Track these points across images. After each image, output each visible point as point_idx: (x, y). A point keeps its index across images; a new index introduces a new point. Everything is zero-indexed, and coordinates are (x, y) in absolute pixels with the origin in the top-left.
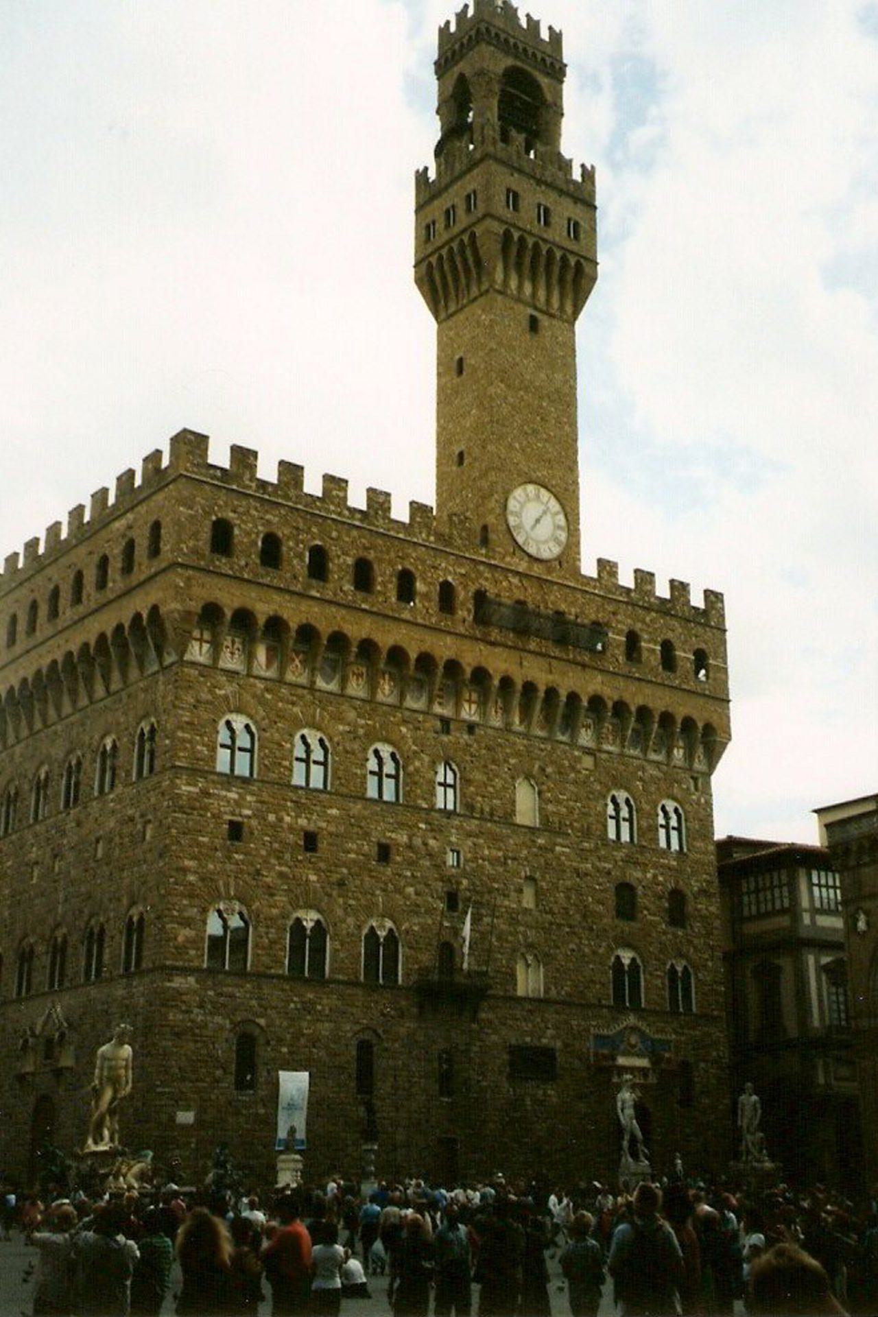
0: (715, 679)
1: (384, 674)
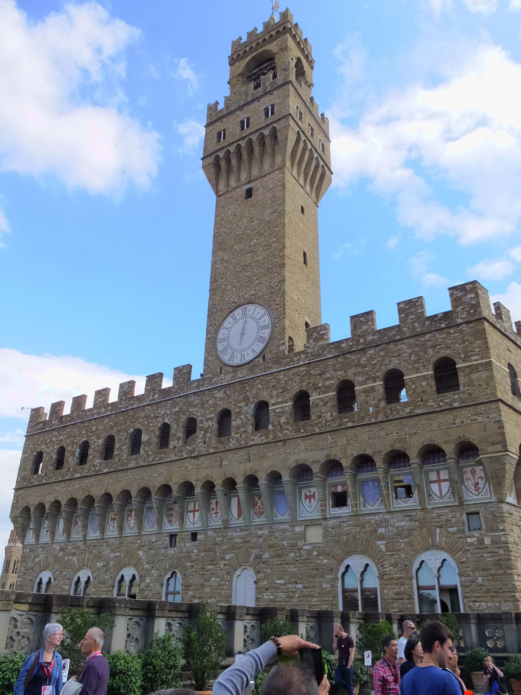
0: (470, 383)
1: (131, 511)
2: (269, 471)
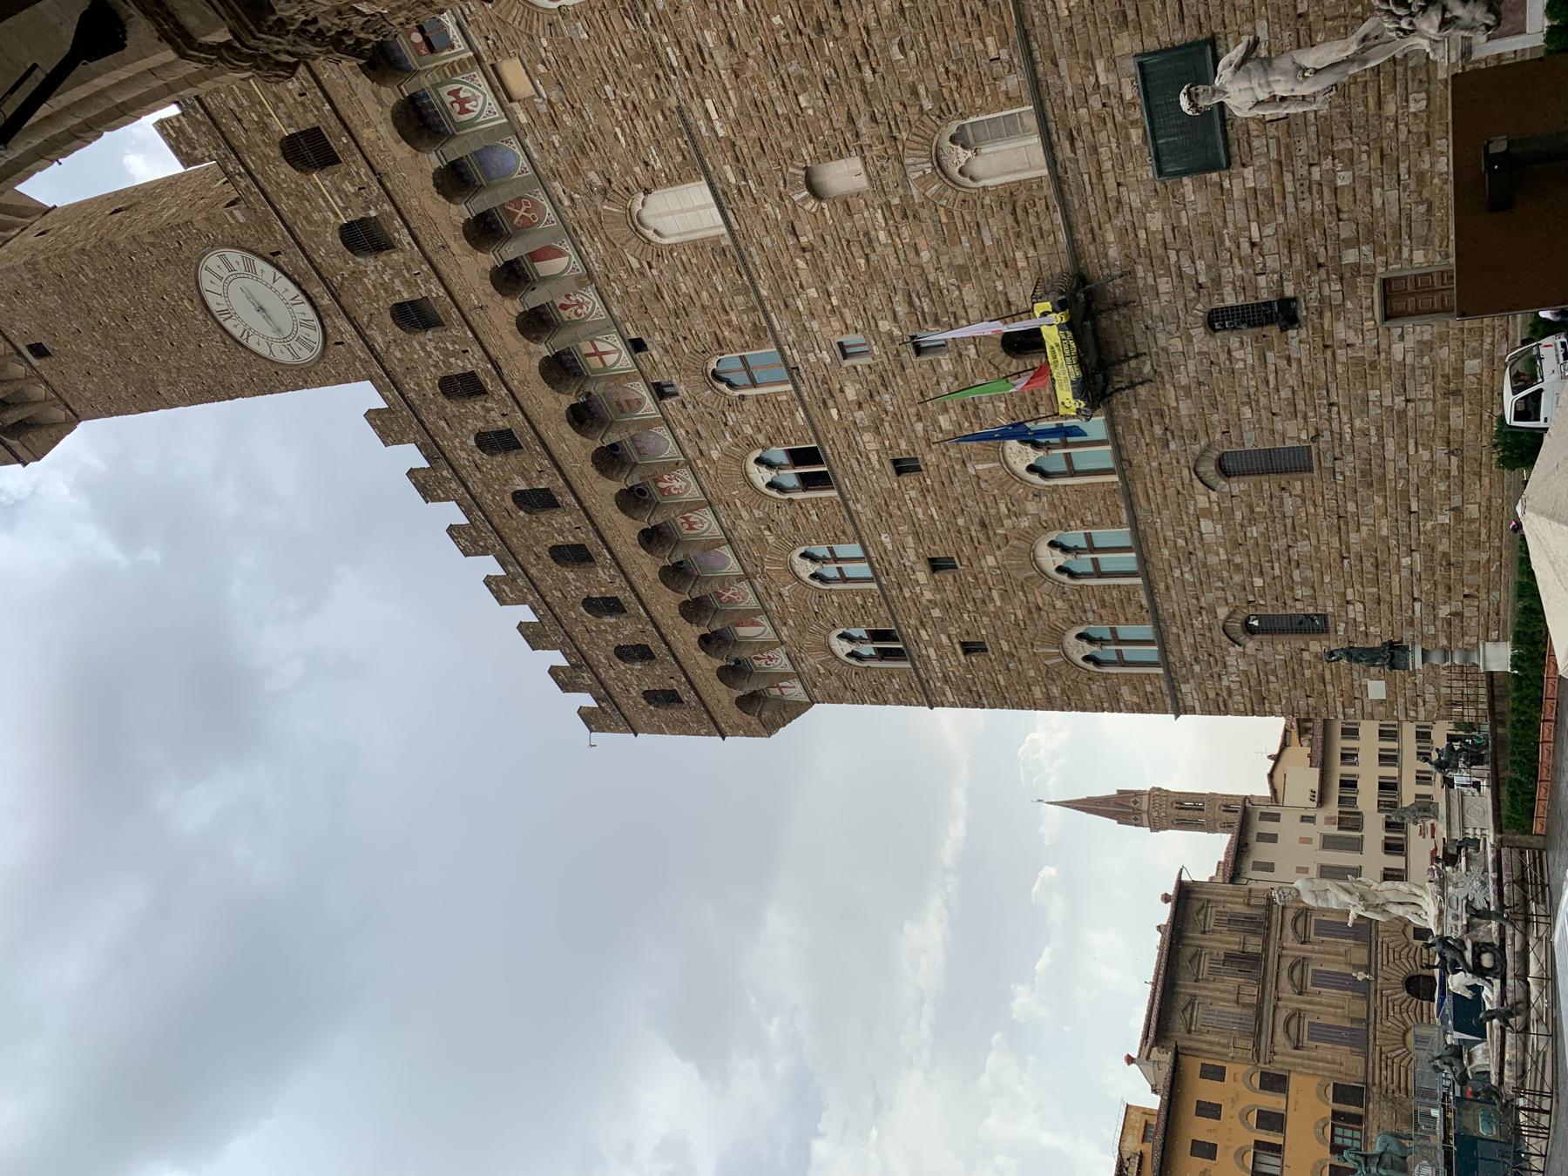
1: (662, 490)
2: (440, 198)
